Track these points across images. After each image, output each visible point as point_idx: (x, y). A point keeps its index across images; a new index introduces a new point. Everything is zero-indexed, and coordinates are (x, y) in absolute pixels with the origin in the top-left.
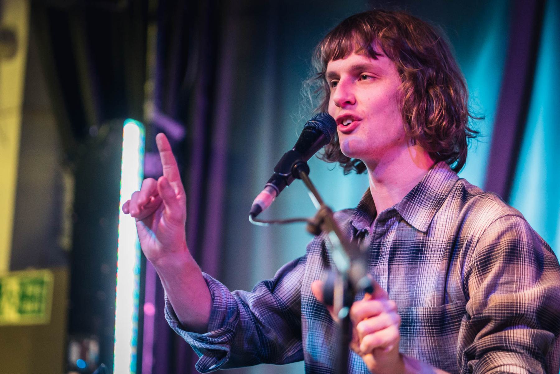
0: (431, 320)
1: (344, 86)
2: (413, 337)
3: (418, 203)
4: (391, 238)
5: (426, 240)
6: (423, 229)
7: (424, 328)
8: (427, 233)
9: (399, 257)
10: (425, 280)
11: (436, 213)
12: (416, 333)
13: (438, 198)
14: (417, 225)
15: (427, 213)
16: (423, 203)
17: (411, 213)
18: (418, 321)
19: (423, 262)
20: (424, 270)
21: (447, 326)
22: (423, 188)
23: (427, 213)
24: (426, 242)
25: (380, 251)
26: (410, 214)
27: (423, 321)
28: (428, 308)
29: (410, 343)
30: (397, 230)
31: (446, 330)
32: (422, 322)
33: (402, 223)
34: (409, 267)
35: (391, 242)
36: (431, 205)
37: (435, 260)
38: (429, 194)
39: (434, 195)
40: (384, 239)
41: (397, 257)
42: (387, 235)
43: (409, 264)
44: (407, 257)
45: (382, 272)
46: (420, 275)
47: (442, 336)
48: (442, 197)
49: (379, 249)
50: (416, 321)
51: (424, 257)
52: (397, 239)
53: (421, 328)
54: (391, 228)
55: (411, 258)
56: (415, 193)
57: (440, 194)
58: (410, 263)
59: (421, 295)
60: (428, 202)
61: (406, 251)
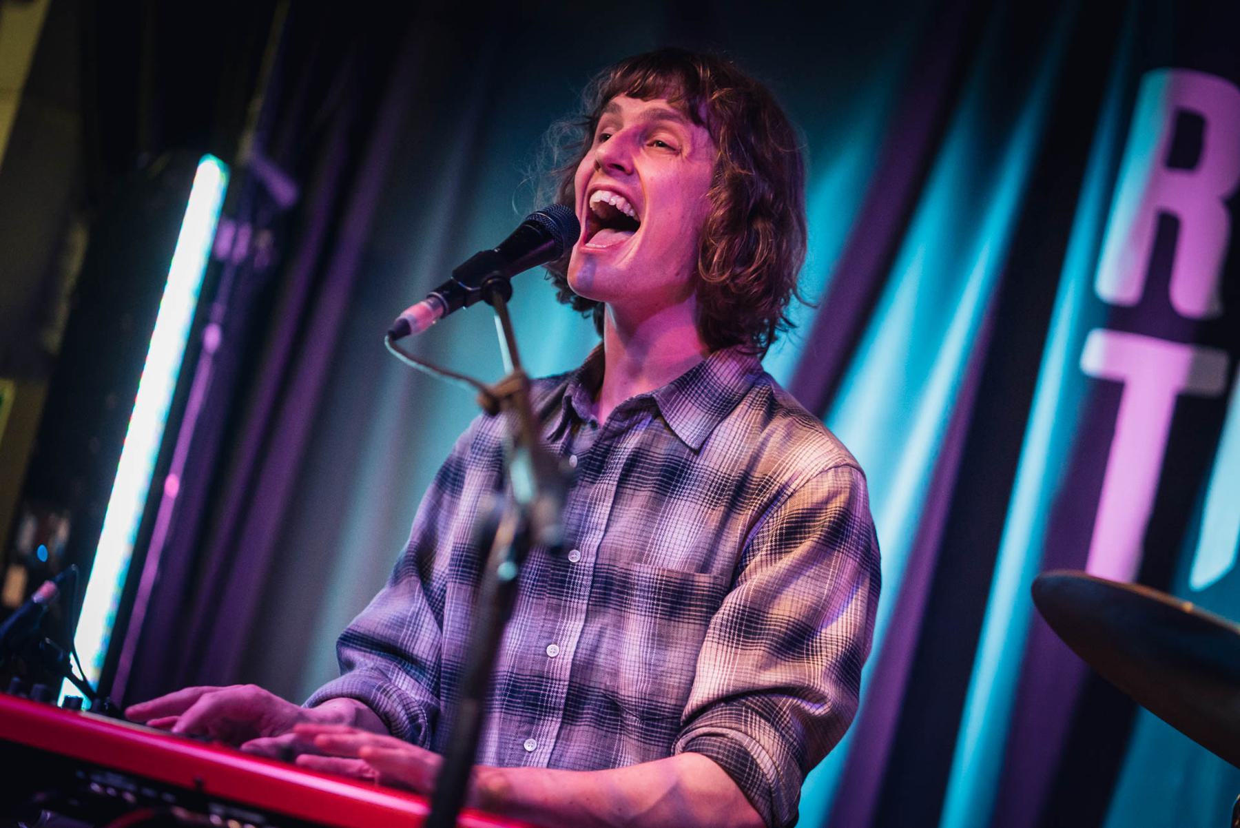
0: (660, 589)
3: (692, 398)
4: (631, 443)
5: (691, 462)
6: (693, 443)
8: (697, 452)
9: (638, 477)
11: (720, 422)
14: (684, 434)
15: (705, 418)
16: (700, 399)
17: (677, 411)
19: (676, 494)
20: (676, 509)
21: (685, 607)
22: (705, 374)
23: (705, 418)
24: (689, 465)
25: (607, 460)
26: (675, 412)
27: (646, 589)
30: (645, 433)
31: (679, 614)
33: (657, 422)
35: (630, 450)
36: (712, 405)
38: (713, 387)
39: (720, 391)
40: (618, 442)
41: (634, 477)
42: (625, 437)
43: (651, 491)
44: (652, 480)
45: (603, 495)
46: (666, 515)
49: (605, 457)
51: (680, 487)
52: (643, 448)
54: (635, 427)
56: (691, 379)
57: (730, 391)
59: (661, 548)
60: (708, 400)
61: (652, 470)
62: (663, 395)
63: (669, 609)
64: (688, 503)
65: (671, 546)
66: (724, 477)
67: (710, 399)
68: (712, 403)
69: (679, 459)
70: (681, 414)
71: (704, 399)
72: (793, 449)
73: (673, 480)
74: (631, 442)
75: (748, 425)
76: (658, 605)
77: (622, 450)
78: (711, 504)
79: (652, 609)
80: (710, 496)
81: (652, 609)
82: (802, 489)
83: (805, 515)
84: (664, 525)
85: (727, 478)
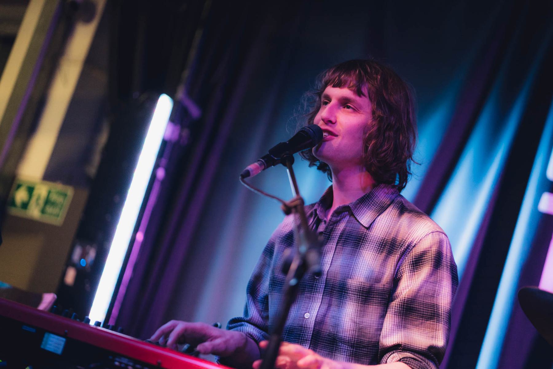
0: (360, 290)
1: (331, 109)
2: (345, 301)
4: (341, 226)
5: (368, 234)
7: (354, 295)
10: (361, 261)
12: (348, 298)
13: (382, 205)
18: (351, 290)
19: (362, 248)
22: (372, 195)
24: (367, 235)
25: (331, 234)
26: (359, 212)
28: (360, 282)
29: (342, 305)
31: (369, 301)
32: (353, 291)
34: (351, 249)
35: (341, 230)
36: (375, 209)
37: (371, 249)
38: (376, 201)
39: (379, 203)
40: (336, 226)
42: (339, 224)
43: (352, 247)
45: (330, 249)
47: (365, 304)
48: (384, 206)
49: (331, 233)
50: (349, 289)
51: (363, 245)
53: (352, 295)
54: (343, 220)
55: (354, 243)
56: (366, 198)
57: (383, 203)
58: (353, 246)
59: (356, 271)
62: (353, 205)
63: (364, 300)
64: (367, 252)
65: (361, 270)
66: (382, 239)
67: (375, 206)
68: (375, 208)
69: (363, 233)
70: (361, 213)
71: (372, 207)
72: (414, 227)
73: (360, 242)
74: (341, 226)
75: (392, 217)
76: (359, 298)
77: (338, 230)
78: (377, 251)
79: (357, 299)
80: (377, 248)
81: (357, 299)
82: (419, 243)
83: (422, 254)
84: (357, 261)
85: (384, 240)
